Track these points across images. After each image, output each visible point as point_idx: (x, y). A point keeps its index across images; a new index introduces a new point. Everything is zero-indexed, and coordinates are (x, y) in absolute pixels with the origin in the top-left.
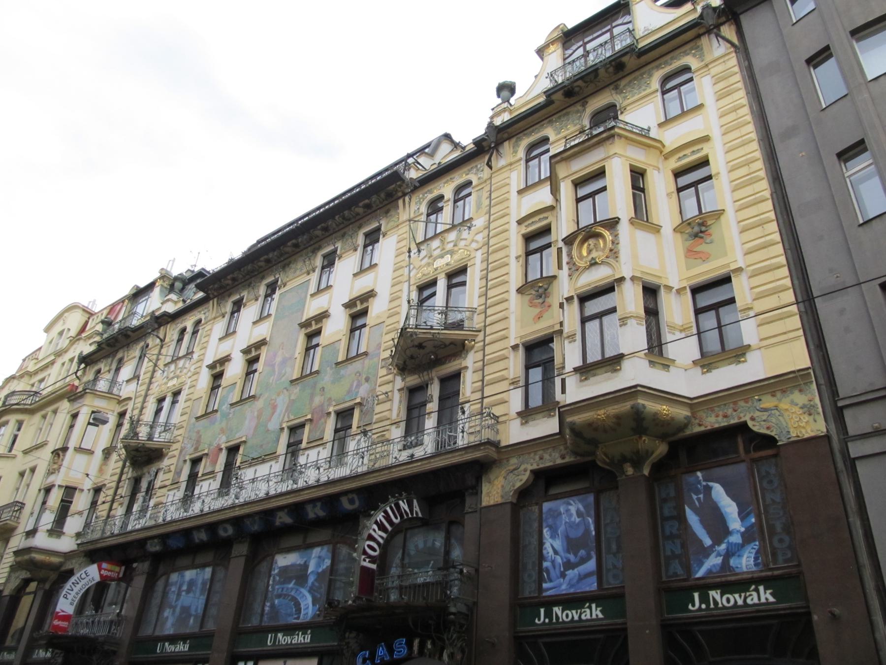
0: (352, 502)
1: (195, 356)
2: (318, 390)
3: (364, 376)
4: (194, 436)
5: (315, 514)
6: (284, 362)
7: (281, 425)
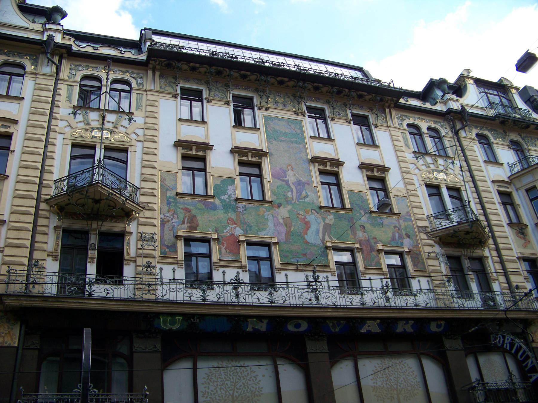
0: (439, 326)
1: (139, 119)
2: (357, 225)
3: (404, 233)
4: (181, 214)
5: (404, 329)
6: (299, 183)
7: (323, 240)
